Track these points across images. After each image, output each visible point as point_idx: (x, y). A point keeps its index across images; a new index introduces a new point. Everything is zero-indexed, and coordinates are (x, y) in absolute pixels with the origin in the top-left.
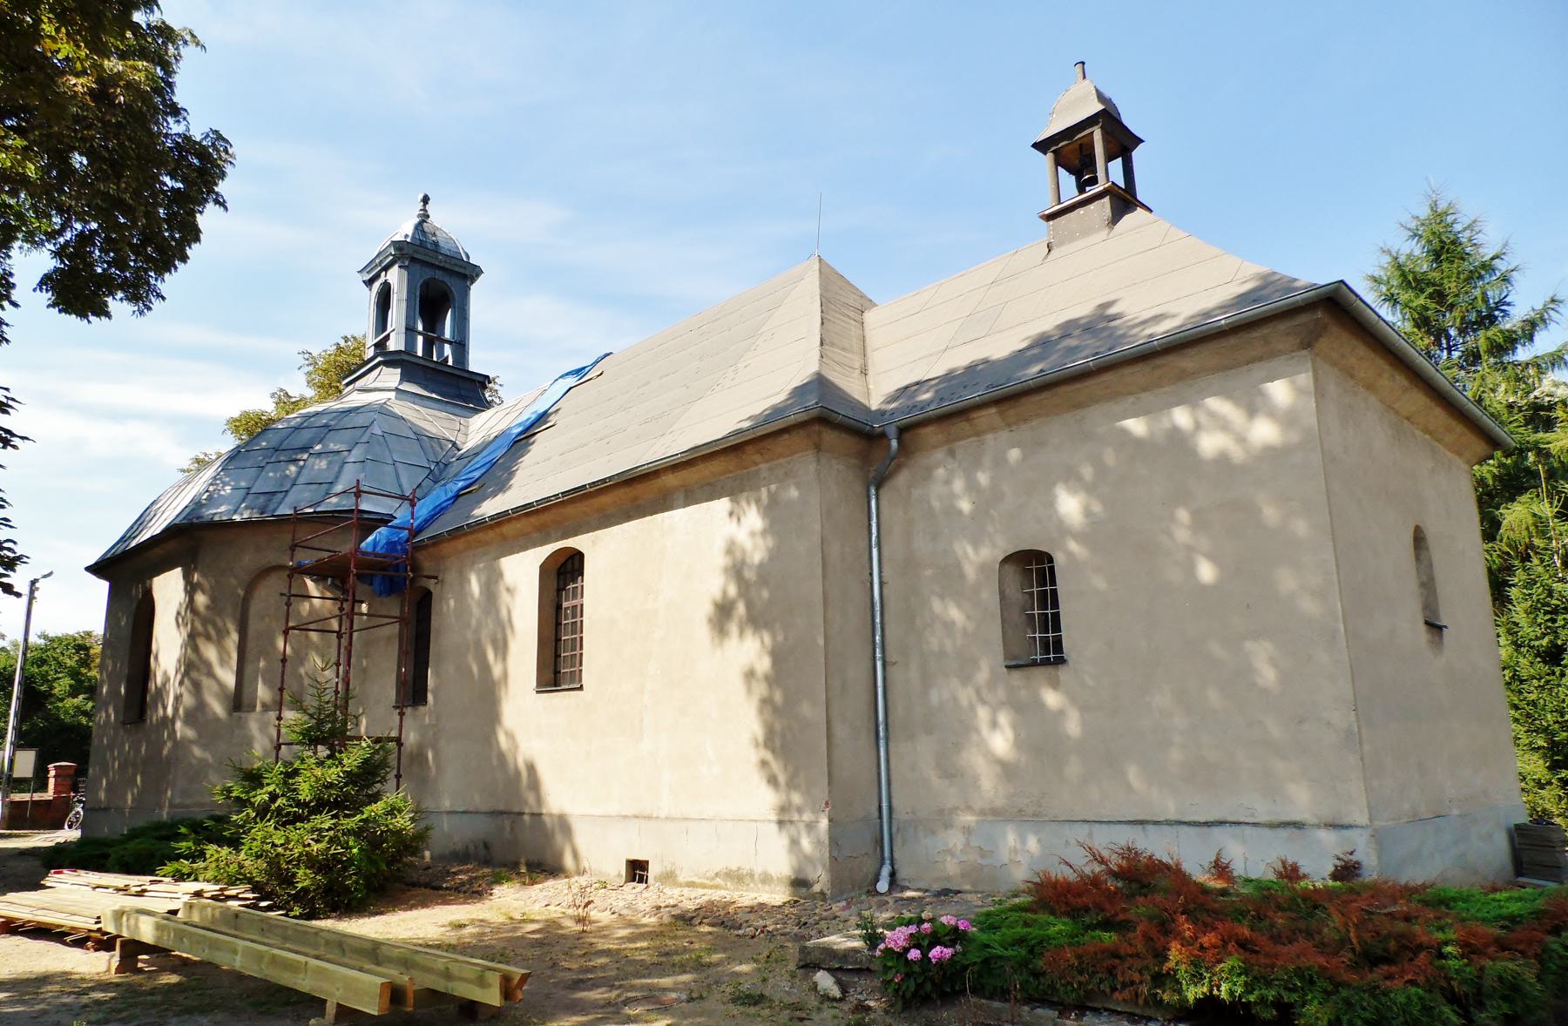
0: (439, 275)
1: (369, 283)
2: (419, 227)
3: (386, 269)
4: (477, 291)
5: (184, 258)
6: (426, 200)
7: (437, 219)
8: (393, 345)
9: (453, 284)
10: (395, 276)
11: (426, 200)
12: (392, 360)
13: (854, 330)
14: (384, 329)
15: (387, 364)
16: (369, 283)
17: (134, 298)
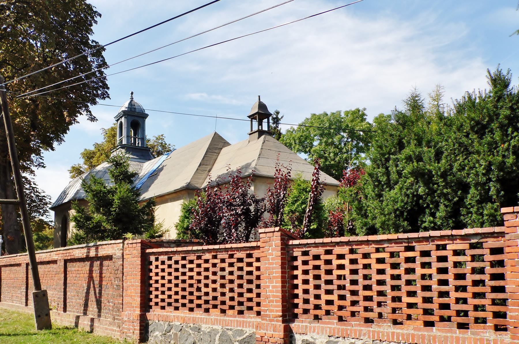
0: (136, 118)
1: (117, 121)
2: (131, 104)
3: (121, 117)
4: (147, 121)
5: (69, 129)
6: (132, 93)
7: (136, 100)
8: (124, 142)
9: (140, 120)
10: (123, 120)
11: (132, 93)
12: (123, 147)
13: (214, 157)
14: (122, 136)
15: (122, 148)
16: (117, 121)
17: (58, 141)
